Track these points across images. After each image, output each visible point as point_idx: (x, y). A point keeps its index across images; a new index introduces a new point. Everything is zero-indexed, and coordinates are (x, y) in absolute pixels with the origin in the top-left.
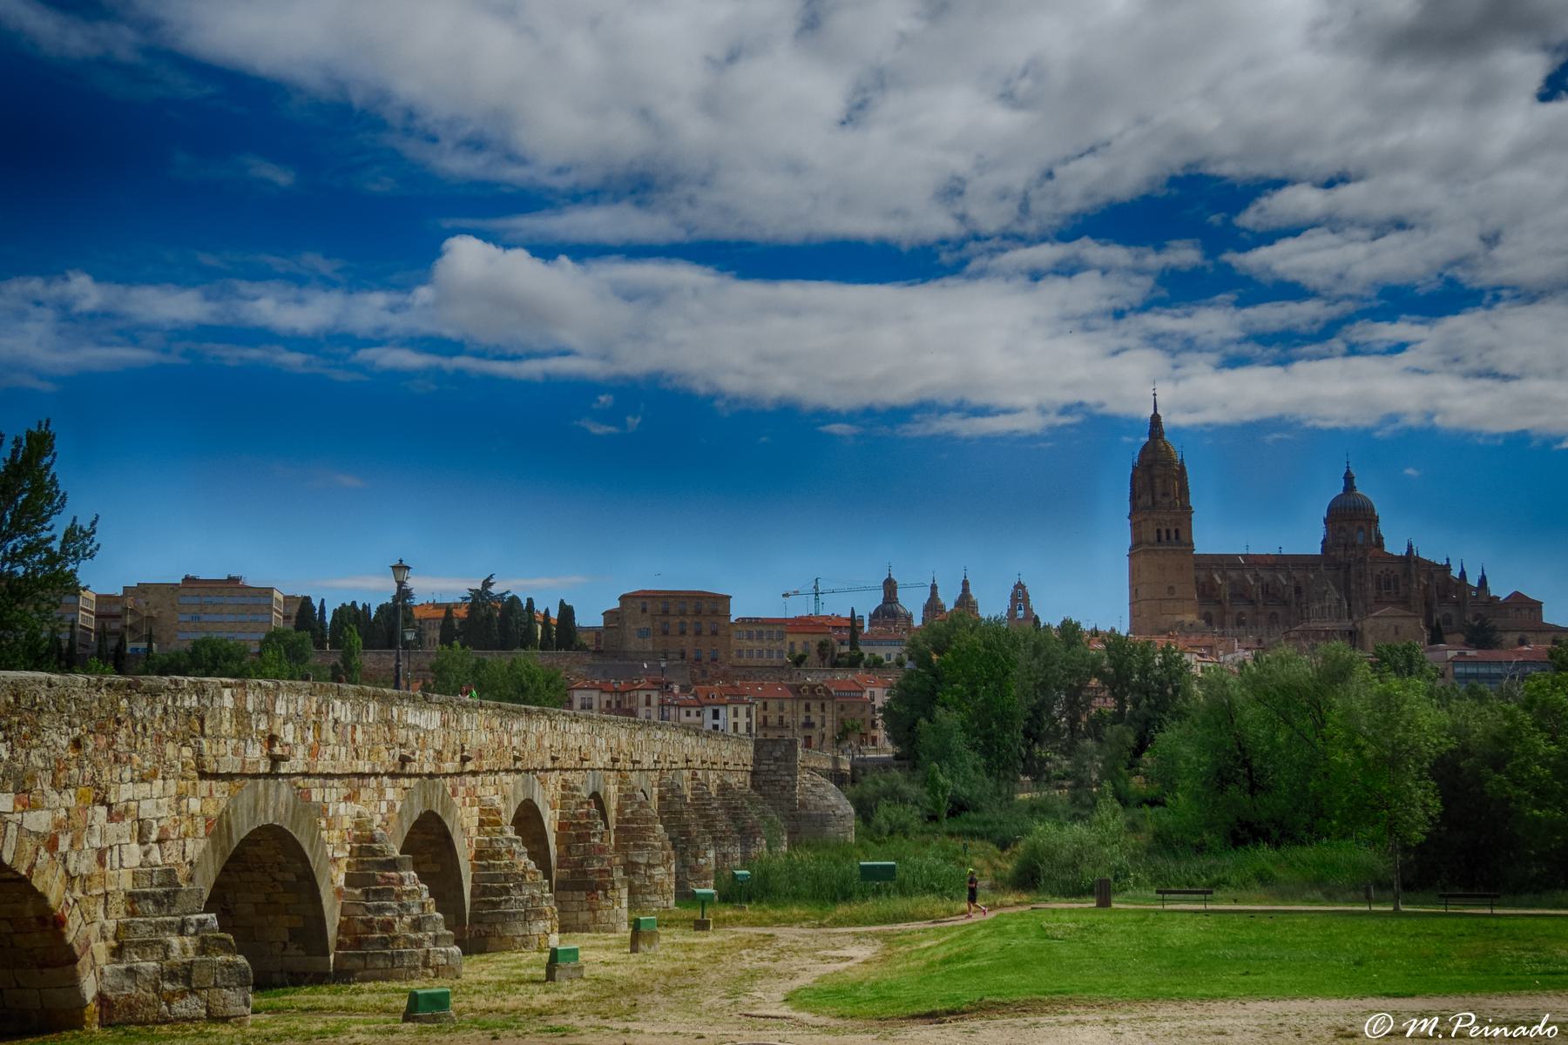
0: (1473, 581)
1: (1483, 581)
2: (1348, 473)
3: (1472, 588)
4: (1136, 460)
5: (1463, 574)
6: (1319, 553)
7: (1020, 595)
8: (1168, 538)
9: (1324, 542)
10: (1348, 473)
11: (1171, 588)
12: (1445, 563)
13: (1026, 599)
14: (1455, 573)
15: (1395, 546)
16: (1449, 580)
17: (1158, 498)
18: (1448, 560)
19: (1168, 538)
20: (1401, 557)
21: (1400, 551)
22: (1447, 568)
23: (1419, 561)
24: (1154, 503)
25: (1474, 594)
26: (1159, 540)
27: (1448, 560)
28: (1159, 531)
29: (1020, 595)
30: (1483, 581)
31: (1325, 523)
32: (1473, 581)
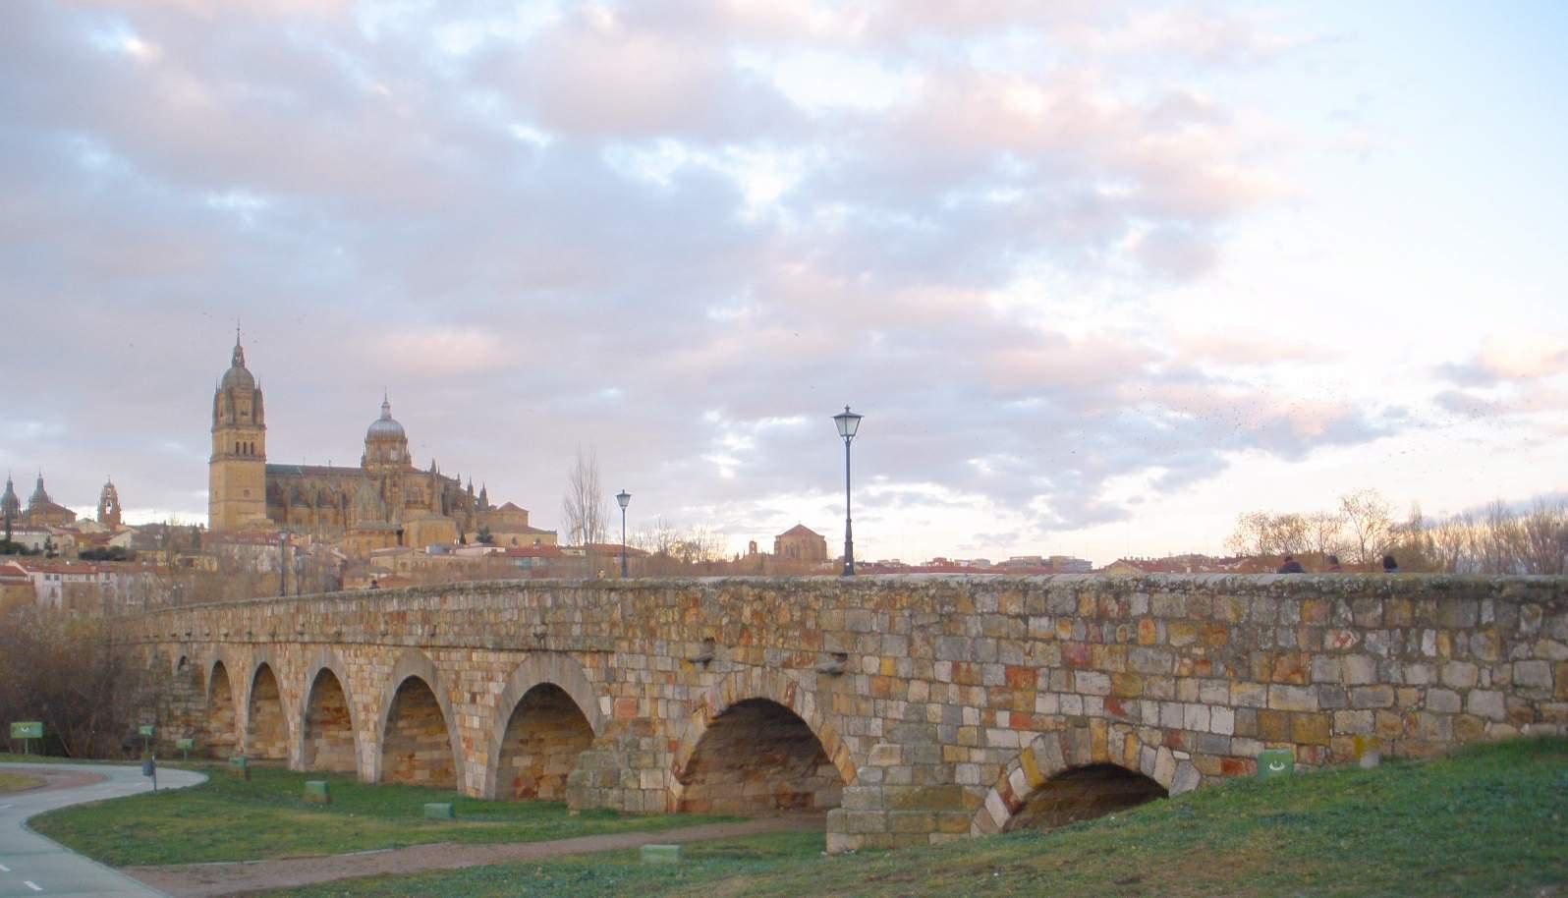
0: (477, 494)
1: (483, 493)
2: (386, 403)
3: (477, 499)
4: (220, 383)
5: (470, 488)
6: (359, 466)
7: (110, 498)
8: (245, 451)
9: (364, 458)
10: (386, 403)
11: (247, 493)
12: (456, 478)
13: (115, 500)
14: (464, 487)
15: (420, 462)
16: (459, 492)
17: (238, 416)
18: (458, 476)
19: (245, 451)
20: (426, 472)
21: (426, 467)
22: (457, 483)
23: (439, 476)
24: (234, 420)
25: (476, 503)
26: (237, 450)
27: (458, 476)
28: (237, 444)
29: (110, 498)
30: (483, 493)
31: (366, 442)
32: (477, 494)
